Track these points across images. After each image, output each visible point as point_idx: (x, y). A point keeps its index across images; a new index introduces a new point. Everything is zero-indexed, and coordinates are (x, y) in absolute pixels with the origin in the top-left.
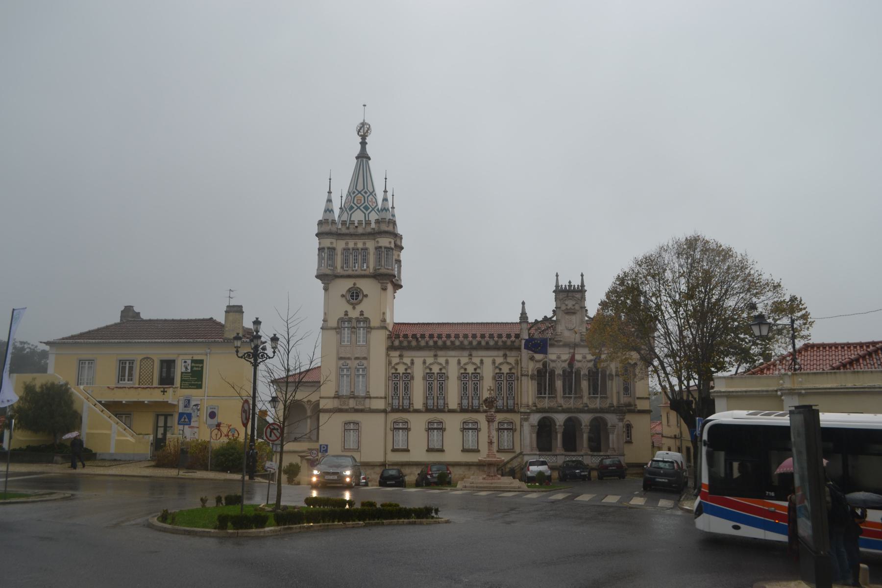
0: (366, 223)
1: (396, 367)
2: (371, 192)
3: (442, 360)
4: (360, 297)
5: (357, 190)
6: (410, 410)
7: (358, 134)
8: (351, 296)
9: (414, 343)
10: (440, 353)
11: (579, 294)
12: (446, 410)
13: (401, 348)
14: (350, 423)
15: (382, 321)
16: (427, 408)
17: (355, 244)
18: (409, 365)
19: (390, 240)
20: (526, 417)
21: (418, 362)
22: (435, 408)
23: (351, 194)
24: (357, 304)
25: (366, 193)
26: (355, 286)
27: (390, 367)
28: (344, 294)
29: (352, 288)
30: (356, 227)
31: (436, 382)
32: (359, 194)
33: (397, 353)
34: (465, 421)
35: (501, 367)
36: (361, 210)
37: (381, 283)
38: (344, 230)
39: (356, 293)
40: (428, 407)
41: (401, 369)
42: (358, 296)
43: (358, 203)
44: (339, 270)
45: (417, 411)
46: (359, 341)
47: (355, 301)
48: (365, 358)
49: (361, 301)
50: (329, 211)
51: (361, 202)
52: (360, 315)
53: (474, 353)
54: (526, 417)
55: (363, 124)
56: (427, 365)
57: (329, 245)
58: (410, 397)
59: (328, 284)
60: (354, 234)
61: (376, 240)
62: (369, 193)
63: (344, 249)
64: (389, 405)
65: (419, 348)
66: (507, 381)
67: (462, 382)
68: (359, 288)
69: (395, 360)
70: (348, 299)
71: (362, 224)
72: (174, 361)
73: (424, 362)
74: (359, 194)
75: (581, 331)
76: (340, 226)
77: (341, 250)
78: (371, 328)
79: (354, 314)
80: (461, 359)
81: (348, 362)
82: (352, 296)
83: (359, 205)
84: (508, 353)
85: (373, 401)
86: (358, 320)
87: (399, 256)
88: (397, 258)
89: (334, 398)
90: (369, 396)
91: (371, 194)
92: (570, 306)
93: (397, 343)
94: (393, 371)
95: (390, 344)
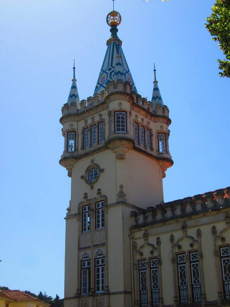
1: (142, 250)
3: (192, 232)
4: (98, 176)
7: (109, 25)
10: (189, 223)
13: (145, 225)
16: (180, 302)
17: (93, 119)
18: (156, 246)
19: (119, 101)
22: (189, 302)
24: (95, 183)
25: (110, 69)
27: (134, 251)
28: (83, 175)
29: (90, 166)
31: (188, 263)
32: (104, 74)
38: (83, 110)
39: (95, 171)
40: (182, 301)
41: (147, 254)
42: (96, 174)
44: (80, 152)
47: (94, 180)
48: (103, 244)
50: (73, 96)
51: (104, 80)
55: (114, 14)
56: (175, 242)
58: (159, 289)
59: (71, 169)
60: (90, 109)
63: (84, 129)
65: (164, 221)
67: (222, 259)
69: (140, 242)
70: (87, 179)
73: (172, 239)
74: (104, 73)
76: (79, 107)
77: (82, 131)
79: (93, 195)
81: (89, 252)
83: (101, 83)
85: (113, 297)
87: (161, 127)
88: (159, 129)
89: (75, 297)
90: (106, 292)
93: (141, 220)
94: (138, 257)
95: (133, 223)
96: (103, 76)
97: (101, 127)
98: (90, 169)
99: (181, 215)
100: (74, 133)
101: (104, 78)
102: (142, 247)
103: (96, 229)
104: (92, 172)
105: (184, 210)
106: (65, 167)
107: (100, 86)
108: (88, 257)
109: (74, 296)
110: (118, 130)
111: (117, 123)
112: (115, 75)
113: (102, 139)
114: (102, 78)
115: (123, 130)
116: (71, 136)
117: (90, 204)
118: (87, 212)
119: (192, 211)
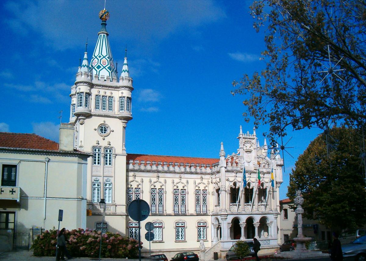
4: (108, 132)
5: (101, 54)
8: (101, 130)
10: (160, 175)
11: (253, 140)
12: (165, 214)
14: (100, 223)
20: (225, 217)
21: (146, 180)
23: (98, 57)
30: (105, 80)
32: (104, 58)
34: (177, 221)
35: (199, 185)
37: (123, 122)
39: (105, 128)
42: (105, 130)
43: (104, 65)
47: (103, 133)
51: (106, 64)
53: (183, 175)
54: (225, 217)
59: (84, 119)
61: (121, 92)
63: (96, 95)
66: (203, 195)
68: (107, 125)
69: (131, 179)
72: (15, 166)
74: (104, 58)
75: (254, 163)
78: (116, 155)
79: (103, 144)
80: (174, 179)
83: (104, 66)
84: (203, 176)
86: (106, 149)
92: (248, 148)
97: (111, 100)
107: (103, 67)
108: (98, 181)
112: (126, 72)
117: (100, 148)
118: (97, 153)
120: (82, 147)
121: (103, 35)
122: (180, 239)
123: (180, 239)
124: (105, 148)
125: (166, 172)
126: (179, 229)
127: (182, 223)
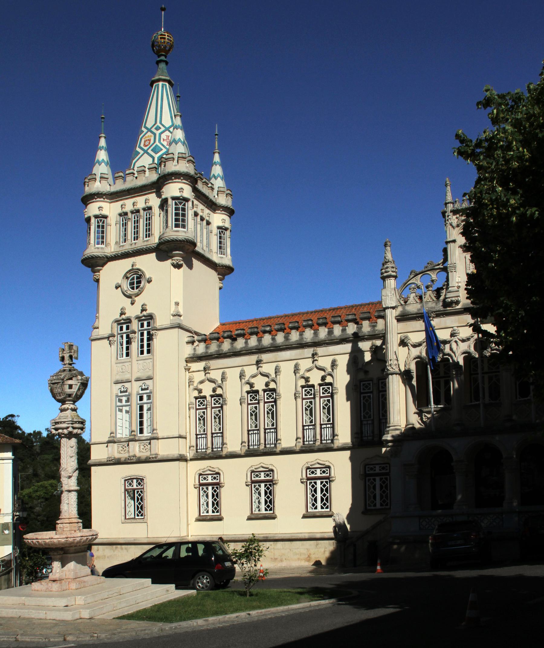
0: (149, 169)
2: (167, 126)
4: (142, 285)
6: (221, 454)
9: (226, 346)
10: (265, 357)
12: (278, 450)
15: (174, 316)
24: (137, 295)
25: (158, 128)
26: (134, 267)
29: (130, 271)
32: (149, 134)
33: (201, 365)
36: (148, 154)
39: (137, 278)
42: (139, 282)
43: (146, 146)
45: (233, 456)
46: (142, 353)
49: (143, 289)
51: (150, 143)
52: (142, 311)
57: (97, 212)
62: (163, 129)
63: (120, 215)
64: (192, 448)
68: (139, 270)
71: (145, 171)
74: (149, 132)
81: (127, 385)
82: (132, 284)
83: (146, 148)
88: (221, 224)
89: (109, 442)
90: (155, 435)
91: (167, 129)
96: (148, 136)
98: (131, 275)
99: (256, 346)
100: (104, 220)
101: (150, 140)
102: (202, 382)
103: (138, 356)
104: (133, 279)
105: (261, 340)
106: (89, 267)
108: (126, 391)
109: (106, 439)
110: (177, 226)
111: (175, 216)
113: (149, 234)
114: (146, 140)
115: (184, 227)
116: (101, 224)
119: (272, 342)
120: (98, 328)
121: (156, 86)
122: (319, 509)
123: (319, 509)
124: (138, 318)
125: (275, 348)
126: (315, 483)
127: (323, 469)
